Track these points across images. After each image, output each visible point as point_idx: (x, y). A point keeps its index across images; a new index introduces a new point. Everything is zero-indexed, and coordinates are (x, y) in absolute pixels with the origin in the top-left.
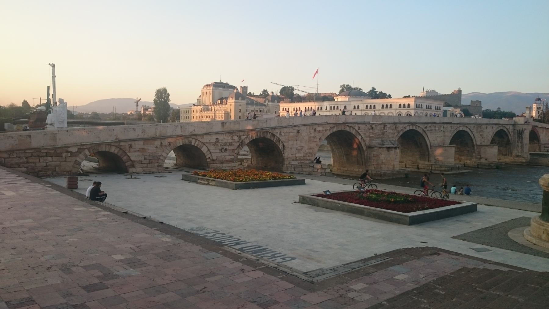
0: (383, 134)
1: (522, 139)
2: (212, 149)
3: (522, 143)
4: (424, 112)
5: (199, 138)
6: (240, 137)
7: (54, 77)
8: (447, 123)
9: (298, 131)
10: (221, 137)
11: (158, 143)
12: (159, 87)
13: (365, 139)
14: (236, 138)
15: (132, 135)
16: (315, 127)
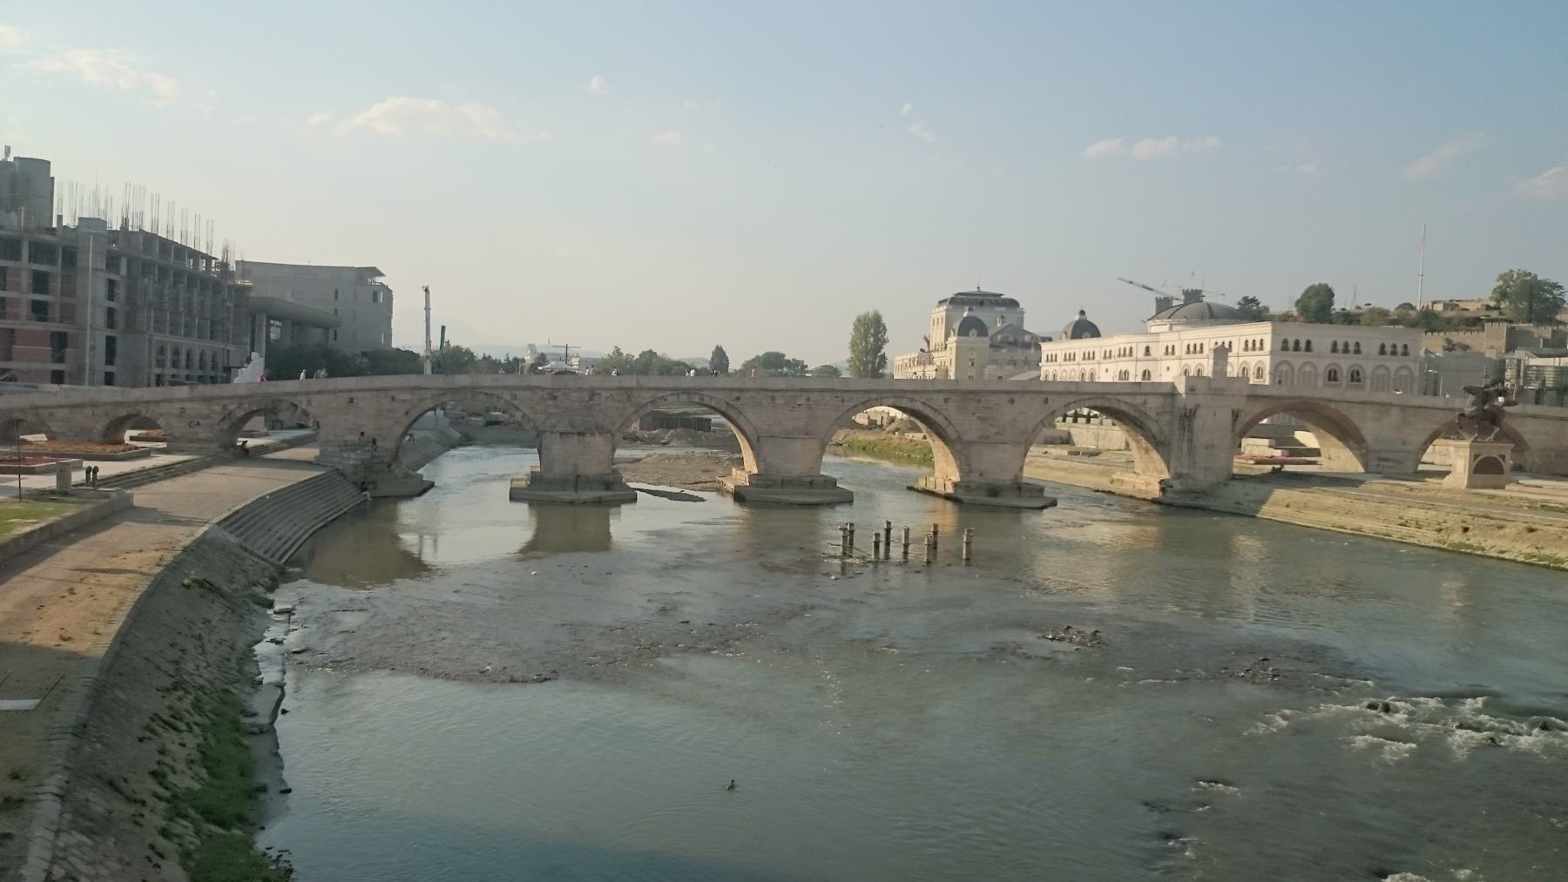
0: (589, 408)
1: (1191, 431)
2: (174, 422)
3: (1190, 441)
4: (1323, 365)
5: (152, 406)
6: (224, 407)
7: (427, 309)
8: (822, 391)
9: (351, 401)
10: (189, 406)
11: (88, 411)
12: (867, 309)
13: (533, 416)
14: (217, 408)
15: (52, 401)
16: (391, 394)
